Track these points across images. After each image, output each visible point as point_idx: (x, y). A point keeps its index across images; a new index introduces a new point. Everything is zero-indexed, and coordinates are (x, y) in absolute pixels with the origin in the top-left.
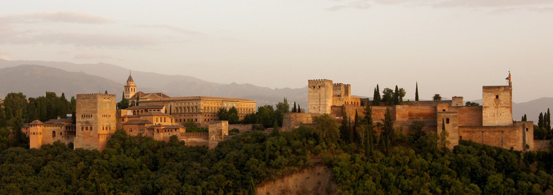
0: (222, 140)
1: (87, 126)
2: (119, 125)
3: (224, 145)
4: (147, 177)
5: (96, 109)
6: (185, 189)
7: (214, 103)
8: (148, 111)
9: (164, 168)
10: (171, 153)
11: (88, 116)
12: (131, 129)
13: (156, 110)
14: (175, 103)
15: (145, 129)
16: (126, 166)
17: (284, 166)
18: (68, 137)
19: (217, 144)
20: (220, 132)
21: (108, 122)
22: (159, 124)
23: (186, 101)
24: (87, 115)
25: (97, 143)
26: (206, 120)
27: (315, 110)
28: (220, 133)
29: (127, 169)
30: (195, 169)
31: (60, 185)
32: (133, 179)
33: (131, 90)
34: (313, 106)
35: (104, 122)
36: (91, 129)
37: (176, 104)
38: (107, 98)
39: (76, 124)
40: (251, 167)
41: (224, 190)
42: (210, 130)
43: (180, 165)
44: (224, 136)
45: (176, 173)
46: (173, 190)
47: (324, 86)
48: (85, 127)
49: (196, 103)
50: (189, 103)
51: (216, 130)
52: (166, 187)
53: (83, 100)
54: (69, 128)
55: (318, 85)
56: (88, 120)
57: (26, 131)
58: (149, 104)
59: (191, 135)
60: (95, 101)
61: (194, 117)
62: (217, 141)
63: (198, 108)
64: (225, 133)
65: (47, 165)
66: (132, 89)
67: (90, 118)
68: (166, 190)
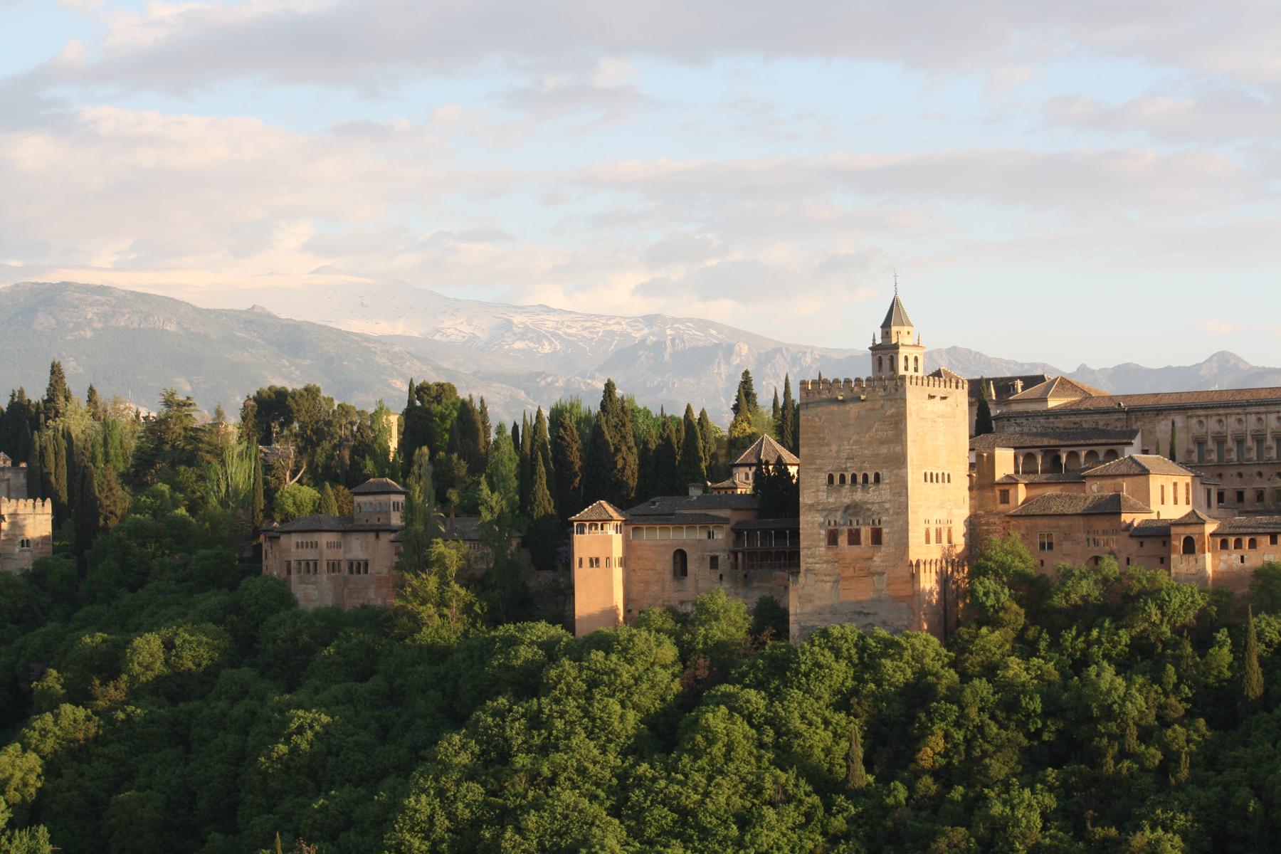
1: (855, 526)
5: (898, 449)
11: (860, 479)
12: (1049, 536)
14: (1191, 417)
18: (746, 576)
24: (854, 477)
25: (904, 605)
31: (789, 799)
36: (877, 538)
37: (1194, 421)
38: (938, 398)
39: (802, 518)
50: (1263, 417)
53: (835, 408)
56: (859, 496)
58: (1061, 425)
60: (893, 410)
66: (906, 359)
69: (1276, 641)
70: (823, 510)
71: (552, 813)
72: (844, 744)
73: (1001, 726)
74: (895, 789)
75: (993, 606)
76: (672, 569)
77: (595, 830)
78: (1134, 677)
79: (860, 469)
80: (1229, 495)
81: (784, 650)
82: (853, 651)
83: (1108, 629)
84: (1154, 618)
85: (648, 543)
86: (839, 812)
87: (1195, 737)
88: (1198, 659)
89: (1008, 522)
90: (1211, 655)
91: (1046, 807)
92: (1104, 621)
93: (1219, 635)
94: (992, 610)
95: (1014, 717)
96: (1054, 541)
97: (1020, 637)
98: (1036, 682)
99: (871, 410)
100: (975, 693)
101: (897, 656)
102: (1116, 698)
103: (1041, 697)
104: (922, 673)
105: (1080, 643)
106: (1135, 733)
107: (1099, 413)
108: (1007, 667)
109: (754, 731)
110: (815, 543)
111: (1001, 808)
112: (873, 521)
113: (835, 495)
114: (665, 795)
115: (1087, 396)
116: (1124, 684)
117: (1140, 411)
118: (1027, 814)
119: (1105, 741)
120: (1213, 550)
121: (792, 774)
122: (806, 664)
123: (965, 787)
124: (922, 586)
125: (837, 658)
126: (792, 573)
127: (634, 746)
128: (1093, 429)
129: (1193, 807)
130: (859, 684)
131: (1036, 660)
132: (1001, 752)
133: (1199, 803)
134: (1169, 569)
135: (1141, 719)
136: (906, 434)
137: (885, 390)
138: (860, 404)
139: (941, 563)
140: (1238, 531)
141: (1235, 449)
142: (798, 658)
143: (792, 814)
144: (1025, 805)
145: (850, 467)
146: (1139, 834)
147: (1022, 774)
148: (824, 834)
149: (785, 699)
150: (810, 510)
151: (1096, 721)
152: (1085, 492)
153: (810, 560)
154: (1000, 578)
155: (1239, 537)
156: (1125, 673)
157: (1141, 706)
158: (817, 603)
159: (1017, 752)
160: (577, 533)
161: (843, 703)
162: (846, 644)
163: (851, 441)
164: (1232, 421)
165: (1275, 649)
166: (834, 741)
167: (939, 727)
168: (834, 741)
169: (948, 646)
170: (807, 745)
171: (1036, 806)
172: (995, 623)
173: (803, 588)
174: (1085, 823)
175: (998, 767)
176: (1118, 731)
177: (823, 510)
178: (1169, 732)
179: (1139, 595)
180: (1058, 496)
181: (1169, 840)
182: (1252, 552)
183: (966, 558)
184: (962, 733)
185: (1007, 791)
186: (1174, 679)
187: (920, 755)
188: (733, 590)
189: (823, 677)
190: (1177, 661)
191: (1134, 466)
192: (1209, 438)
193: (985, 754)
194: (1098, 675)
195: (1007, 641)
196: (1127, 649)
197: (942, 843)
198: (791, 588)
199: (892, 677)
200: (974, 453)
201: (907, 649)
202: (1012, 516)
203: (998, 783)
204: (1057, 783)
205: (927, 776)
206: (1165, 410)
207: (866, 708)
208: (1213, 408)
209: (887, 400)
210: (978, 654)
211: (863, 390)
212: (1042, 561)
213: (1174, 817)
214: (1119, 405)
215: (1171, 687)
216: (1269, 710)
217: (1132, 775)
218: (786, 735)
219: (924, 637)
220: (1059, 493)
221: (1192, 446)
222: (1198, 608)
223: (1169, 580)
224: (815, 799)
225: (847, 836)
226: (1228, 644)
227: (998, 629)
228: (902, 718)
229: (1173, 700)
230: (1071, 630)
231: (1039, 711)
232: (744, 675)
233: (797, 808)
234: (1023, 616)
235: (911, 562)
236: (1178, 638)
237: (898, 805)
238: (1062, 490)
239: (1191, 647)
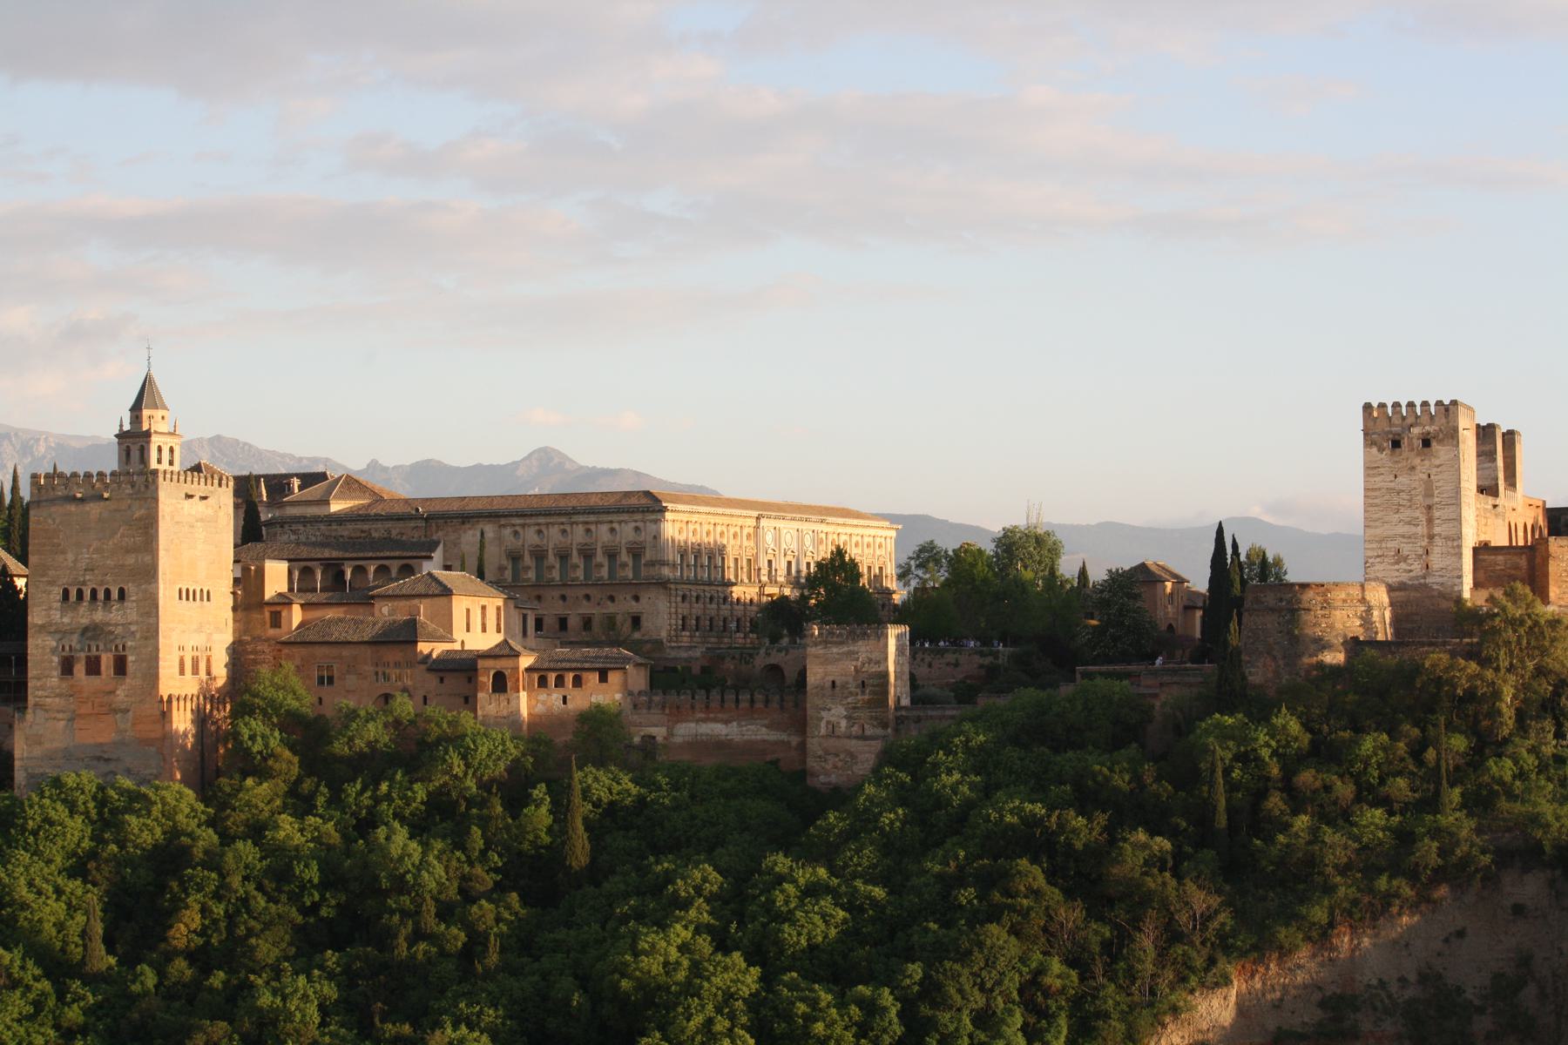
0: (889, 730)
1: (94, 652)
2: (249, 648)
5: (148, 559)
6: (802, 1008)
11: (101, 595)
12: (329, 668)
14: (500, 526)
17: (1329, 870)
23: (575, 518)
24: (94, 593)
25: (153, 749)
27: (1403, 566)
34: (1392, 545)
35: (184, 632)
36: (120, 667)
37: (507, 532)
38: (196, 498)
39: (31, 642)
42: (815, 674)
47: (1453, 438)
49: (633, 524)
50: (593, 527)
51: (850, 679)
53: (72, 508)
55: (1416, 431)
58: (346, 533)
59: (693, 707)
60: (143, 512)
61: (624, 606)
62: (857, 738)
63: (648, 555)
66: (160, 449)
69: (606, 801)
70: (56, 632)
72: (80, 918)
73: (270, 899)
74: (142, 974)
75: (260, 753)
78: (432, 841)
79: (102, 583)
80: (549, 622)
81: (7, 802)
82: (91, 805)
83: (400, 783)
84: (456, 770)
86: (74, 1001)
87: (506, 915)
88: (510, 821)
89: (280, 650)
90: (526, 815)
91: (325, 999)
92: (395, 773)
93: (536, 792)
94: (259, 757)
95: (286, 888)
97: (293, 791)
98: (312, 845)
99: (116, 510)
100: (238, 858)
101: (144, 812)
102: (410, 867)
103: (319, 864)
104: (174, 833)
105: (366, 799)
106: (433, 910)
107: (392, 519)
108: (277, 827)
111: (271, 999)
112: (116, 646)
113: (70, 614)
115: (378, 498)
116: (420, 849)
117: (443, 518)
118: (302, 1005)
119: (396, 918)
120: (529, 688)
121: (17, 954)
122: (34, 820)
123: (226, 973)
124: (174, 727)
125: (72, 813)
126: (18, 708)
128: (385, 539)
129: (504, 1001)
130: (98, 843)
131: (313, 819)
132: (270, 930)
133: (511, 995)
134: (475, 711)
135: (440, 893)
136: (158, 541)
137: (133, 486)
138: (102, 503)
139: (198, 699)
140: (560, 665)
141: (558, 566)
142: (25, 812)
143: (17, 1002)
144: (299, 995)
145: (89, 580)
146: (438, 1033)
147: (295, 957)
148: (57, 1027)
149: (9, 862)
150: (40, 632)
151: (386, 894)
152: (373, 616)
153: (40, 693)
154: (270, 719)
155: (559, 673)
156: (421, 836)
157: (441, 877)
158: (47, 745)
159: (290, 931)
161: (79, 868)
162: (82, 797)
163: (91, 550)
164: (554, 532)
165: (604, 809)
166: (68, 914)
167: (194, 900)
168: (68, 914)
169: (204, 798)
170: (36, 919)
171: (312, 996)
172: (263, 773)
173: (31, 726)
174: (372, 1018)
175: (266, 949)
176: (412, 907)
177: (56, 632)
178: (475, 909)
179: (438, 741)
180: (341, 620)
181: (475, 1040)
182: (577, 692)
183: (228, 693)
184: (222, 906)
185: (278, 979)
186: (480, 843)
187: (172, 932)
189: (55, 836)
190: (484, 822)
191: (433, 584)
192: (526, 552)
193: (250, 932)
194: (388, 838)
195: (277, 795)
196: (423, 808)
197: (200, 1039)
198: (16, 726)
199: (138, 837)
200: (239, 566)
201: (155, 803)
203: (267, 969)
204: (339, 969)
205: (181, 959)
206: (472, 517)
207: (107, 875)
208: (531, 515)
209: (136, 499)
210: (241, 811)
211: (107, 487)
212: (320, 699)
213: (481, 1012)
214: (417, 510)
215: (477, 854)
216: (598, 885)
217: (429, 960)
218: (10, 906)
219: (177, 789)
220: (342, 616)
221: (504, 562)
222: (510, 758)
223: (476, 724)
224: (46, 985)
225: (84, 1031)
226: (547, 803)
227: (266, 780)
229: (479, 870)
230: (355, 782)
231: (316, 881)
233: (23, 995)
234: (297, 765)
235: (162, 697)
236: (485, 794)
237: (146, 993)
238: (345, 613)
239: (502, 805)
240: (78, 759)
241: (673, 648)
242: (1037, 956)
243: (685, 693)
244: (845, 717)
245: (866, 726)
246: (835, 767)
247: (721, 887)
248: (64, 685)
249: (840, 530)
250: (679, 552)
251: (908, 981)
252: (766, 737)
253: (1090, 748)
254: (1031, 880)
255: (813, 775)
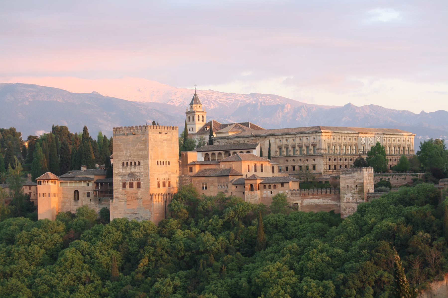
1: (131, 181)
3: (371, 208)
4: (237, 267)
5: (146, 152)
7: (343, 137)
8: (230, 155)
9: (267, 250)
10: (277, 225)
11: (133, 164)
12: (206, 184)
13: (245, 151)
15: (230, 185)
16: (201, 249)
18: (99, 200)
19: (356, 209)
20: (360, 188)
21: (166, 173)
22: (254, 175)
23: (297, 135)
24: (131, 163)
25: (148, 210)
26: (331, 167)
28: (359, 189)
29: (202, 253)
30: (321, 252)
31: (92, 282)
32: (213, 270)
33: (196, 118)
36: (139, 185)
37: (278, 140)
38: (163, 133)
39: (114, 178)
40: (419, 247)
41: (373, 287)
42: (343, 184)
43: (293, 245)
44: (367, 194)
45: (288, 258)
46: (284, 288)
48: (128, 182)
49: (313, 137)
50: (302, 138)
51: (353, 184)
52: (273, 283)
53: (124, 137)
54: (102, 185)
56: (133, 170)
57: (30, 191)
58: (232, 142)
59: (309, 194)
60: (144, 138)
61: (311, 163)
62: (355, 203)
63: (317, 147)
64: (368, 188)
65: (68, 247)
66: (198, 116)
67: (137, 167)
68: (273, 288)
70: (121, 175)
71: (7, 287)
75: (177, 211)
76: (74, 197)
77: (21, 293)
80: (290, 168)
82: (123, 228)
84: (231, 215)
85: (65, 188)
93: (254, 221)
94: (176, 212)
96: (207, 186)
99: (137, 138)
102: (209, 245)
105: (205, 224)
107: (245, 137)
109: (83, 257)
110: (119, 188)
113: (125, 170)
114: (47, 281)
126: (111, 199)
127: (42, 262)
129: (225, 286)
141: (292, 150)
142: (103, 230)
144: (167, 284)
150: (116, 175)
153: (117, 194)
160: (39, 184)
164: (291, 140)
166: (111, 261)
170: (100, 262)
177: (121, 175)
187: (139, 266)
188: (95, 205)
189: (111, 237)
198: (110, 204)
202: (193, 177)
214: (252, 134)
218: (94, 258)
224: (100, 282)
228: (137, 252)
231: (183, 249)
232: (85, 236)
233: (92, 285)
240: (128, 214)
241: (325, 175)
242: (381, 271)
243: (306, 190)
244: (351, 196)
245: (358, 199)
246: (349, 212)
247: (297, 250)
248: (123, 191)
249: (392, 136)
250: (327, 145)
251: (338, 279)
252: (331, 203)
253: (415, 205)
254: (384, 247)
255: (343, 215)
